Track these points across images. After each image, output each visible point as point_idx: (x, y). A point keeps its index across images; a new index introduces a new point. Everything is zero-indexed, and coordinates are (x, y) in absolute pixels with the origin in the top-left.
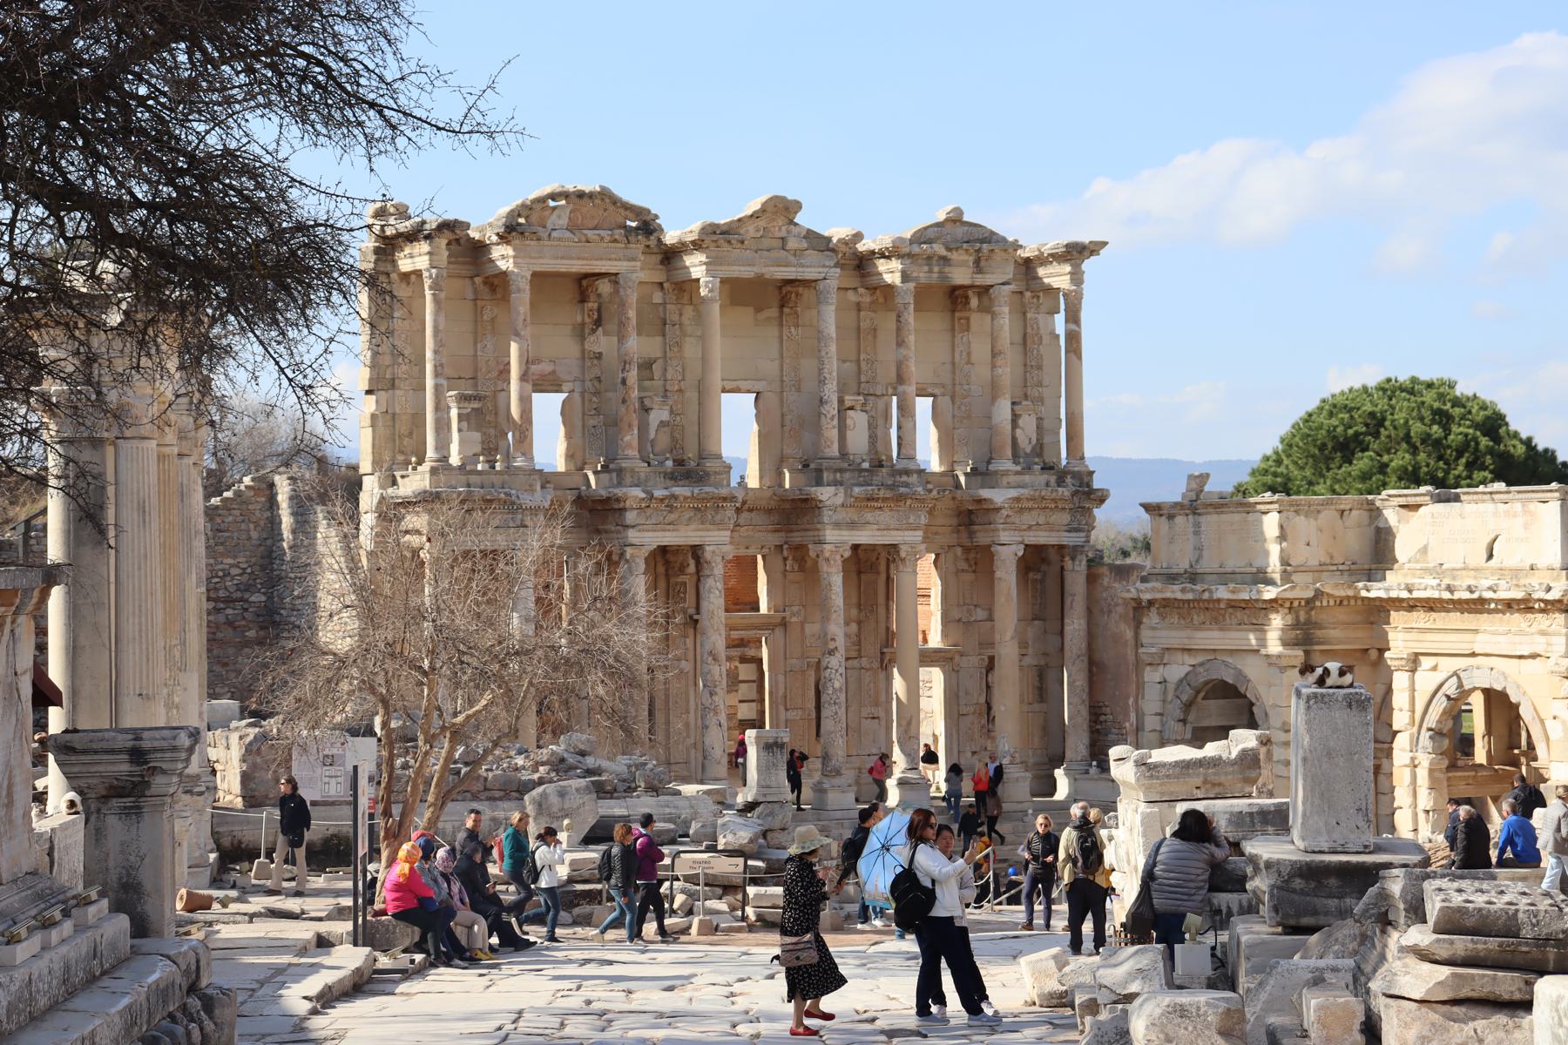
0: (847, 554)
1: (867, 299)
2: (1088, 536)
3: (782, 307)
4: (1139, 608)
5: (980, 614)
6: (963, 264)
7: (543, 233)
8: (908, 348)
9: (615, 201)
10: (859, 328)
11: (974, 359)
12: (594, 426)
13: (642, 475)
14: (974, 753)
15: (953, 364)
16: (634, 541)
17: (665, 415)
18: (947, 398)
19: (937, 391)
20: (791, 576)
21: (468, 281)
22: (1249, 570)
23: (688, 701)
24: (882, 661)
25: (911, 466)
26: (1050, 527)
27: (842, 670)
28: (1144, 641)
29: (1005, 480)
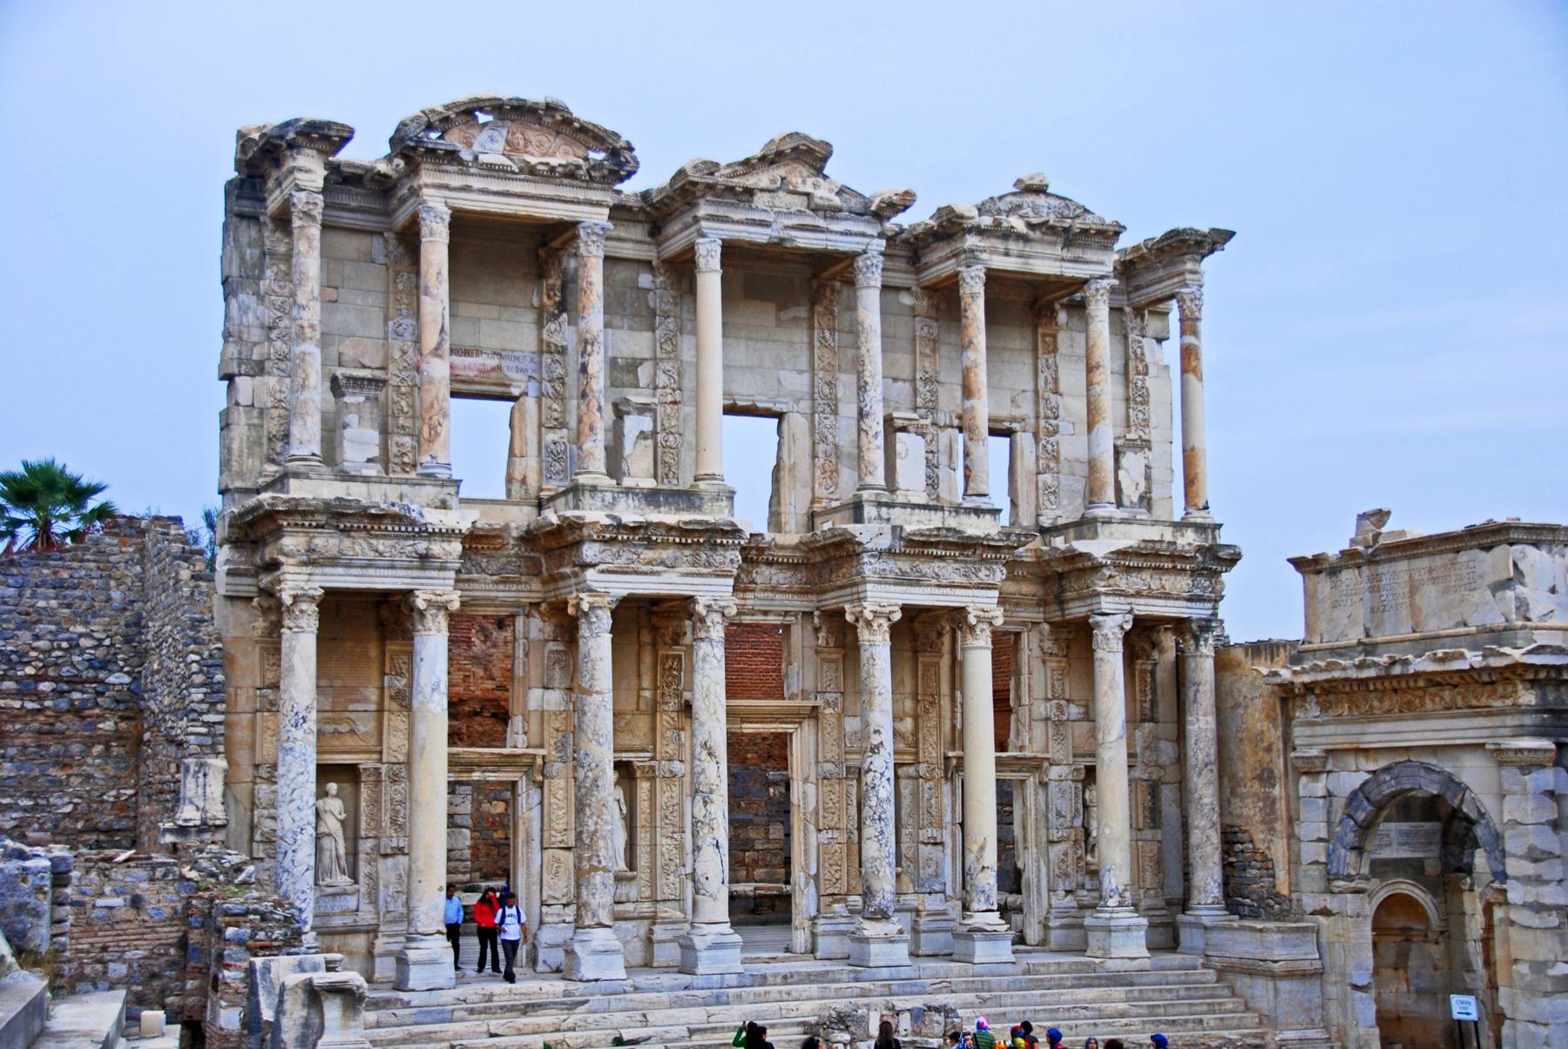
0: (897, 616)
2: (1215, 608)
4: (1288, 696)
5: (1074, 711)
7: (466, 155)
8: (976, 350)
9: (568, 121)
11: (1062, 388)
15: (1036, 392)
16: (594, 585)
17: (646, 423)
19: (1015, 425)
22: (1461, 630)
23: (682, 816)
24: (946, 771)
25: (982, 503)
26: (1167, 596)
27: (890, 774)
28: (1297, 742)
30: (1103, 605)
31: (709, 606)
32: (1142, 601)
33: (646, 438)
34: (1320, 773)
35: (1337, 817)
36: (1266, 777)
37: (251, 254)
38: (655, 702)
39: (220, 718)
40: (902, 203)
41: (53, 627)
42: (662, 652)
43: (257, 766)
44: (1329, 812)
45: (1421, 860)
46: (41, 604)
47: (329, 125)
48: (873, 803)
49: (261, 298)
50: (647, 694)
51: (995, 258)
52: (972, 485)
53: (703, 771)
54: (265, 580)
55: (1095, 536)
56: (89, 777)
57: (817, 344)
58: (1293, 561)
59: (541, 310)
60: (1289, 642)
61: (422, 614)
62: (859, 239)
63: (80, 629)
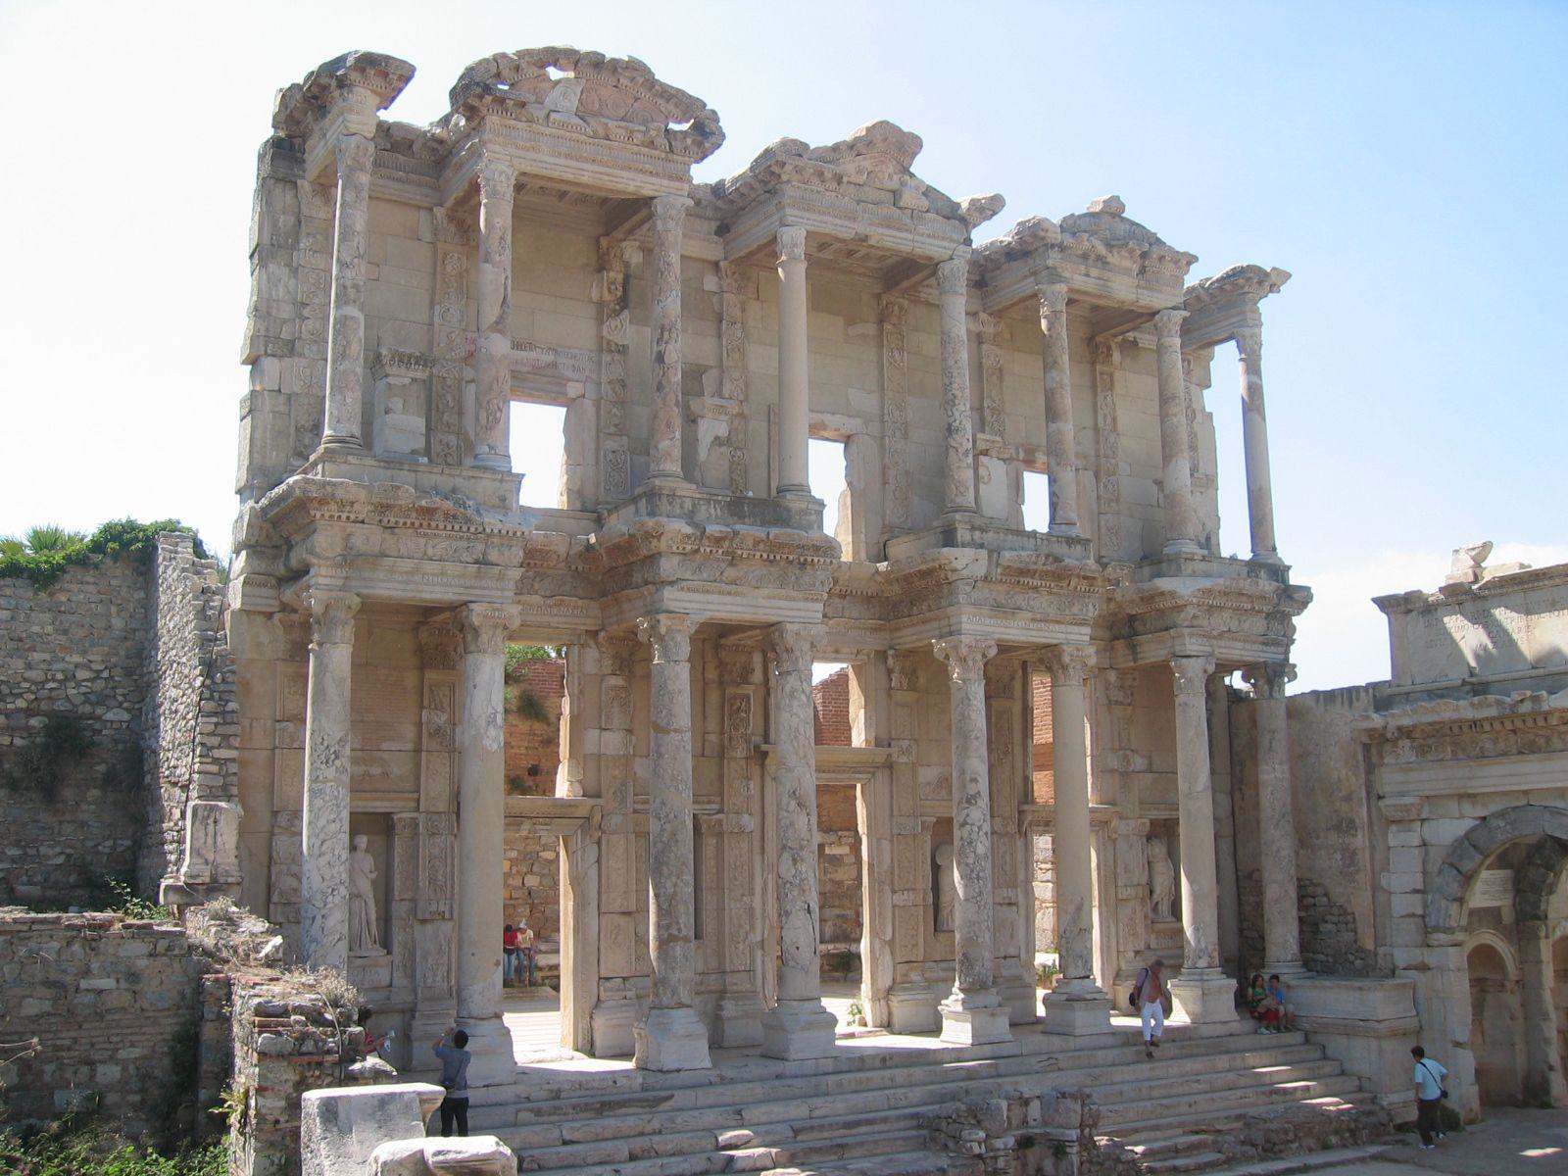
0: (993, 652)
1: (990, 330)
2: (1287, 652)
3: (881, 322)
6: (1127, 272)
10: (980, 366)
11: (1120, 426)
12: (613, 471)
13: (688, 504)
14: (1137, 953)
16: (672, 605)
17: (722, 430)
18: (1090, 474)
20: (899, 696)
21: (424, 216)
23: (752, 877)
24: (1020, 825)
29: (1188, 567)
30: (1188, 647)
31: (798, 634)
32: (1222, 643)
33: (721, 445)
34: (1411, 821)
35: (1433, 868)
36: (1345, 826)
37: (286, 221)
38: (723, 748)
39: (233, 754)
40: (990, 207)
41: (47, 656)
42: (730, 691)
43: (275, 813)
44: (1424, 862)
45: (1498, 909)
46: (36, 629)
47: (387, 59)
48: (971, 861)
49: (294, 271)
50: (713, 738)
51: (1076, 276)
52: (1060, 513)
53: (792, 824)
54: (288, 594)
55: (1178, 573)
56: (83, 824)
57: (886, 364)
58: (1376, 600)
59: (600, 305)
60: (1342, 690)
61: (476, 631)
62: (945, 244)
63: (77, 659)
